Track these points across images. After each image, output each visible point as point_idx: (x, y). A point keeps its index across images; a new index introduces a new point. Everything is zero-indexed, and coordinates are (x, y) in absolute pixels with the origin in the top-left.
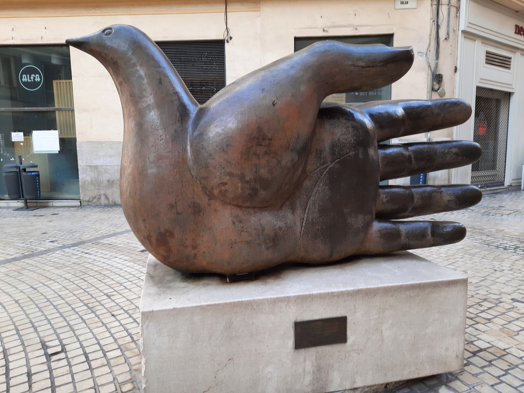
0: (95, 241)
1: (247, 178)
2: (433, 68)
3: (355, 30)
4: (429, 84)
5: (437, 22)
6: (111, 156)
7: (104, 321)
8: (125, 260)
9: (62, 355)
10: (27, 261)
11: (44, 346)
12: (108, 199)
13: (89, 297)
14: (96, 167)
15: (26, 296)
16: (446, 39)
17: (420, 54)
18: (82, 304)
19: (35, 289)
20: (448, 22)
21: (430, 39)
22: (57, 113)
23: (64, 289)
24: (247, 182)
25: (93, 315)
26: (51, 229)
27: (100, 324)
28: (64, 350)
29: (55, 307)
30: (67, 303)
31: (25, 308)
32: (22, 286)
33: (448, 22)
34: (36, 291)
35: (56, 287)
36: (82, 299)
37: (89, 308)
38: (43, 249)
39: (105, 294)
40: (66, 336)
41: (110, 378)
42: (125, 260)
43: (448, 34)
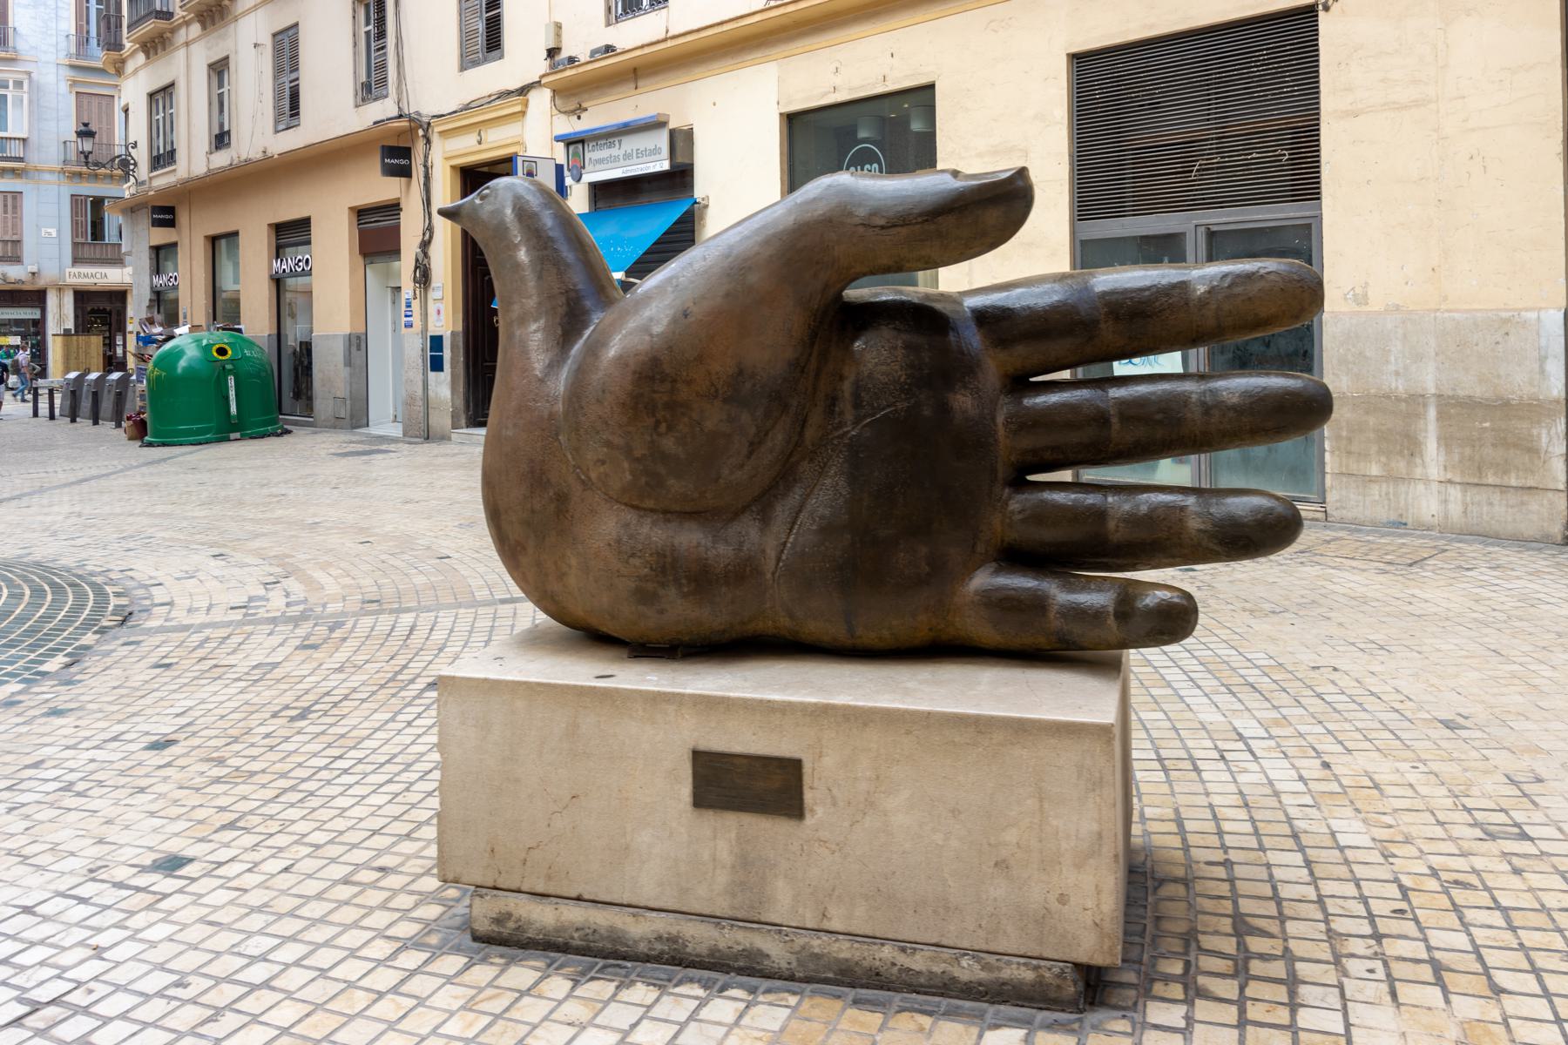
1: (638, 453)
24: (638, 460)
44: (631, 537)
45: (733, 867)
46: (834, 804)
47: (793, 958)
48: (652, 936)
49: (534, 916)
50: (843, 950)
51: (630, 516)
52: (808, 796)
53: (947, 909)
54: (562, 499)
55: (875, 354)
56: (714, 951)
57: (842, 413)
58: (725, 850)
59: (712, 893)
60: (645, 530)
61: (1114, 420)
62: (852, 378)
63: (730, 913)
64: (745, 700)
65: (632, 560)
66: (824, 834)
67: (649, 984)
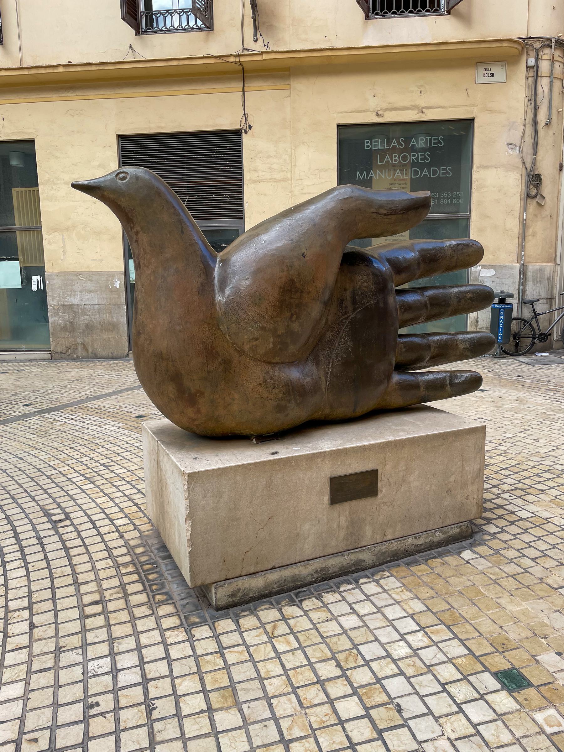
0: (79, 404)
2: (529, 165)
3: (420, 114)
4: (523, 188)
5: (535, 101)
6: (90, 292)
7: (105, 491)
8: (119, 428)
9: (68, 522)
11: (47, 514)
12: (87, 350)
13: (85, 467)
14: (71, 306)
15: (12, 466)
16: (546, 124)
17: (510, 146)
18: (77, 474)
19: (21, 458)
20: (550, 100)
21: (524, 125)
22: (18, 233)
23: (53, 459)
25: (92, 486)
26: (21, 390)
27: (102, 494)
28: (67, 517)
29: (49, 477)
30: (60, 472)
31: (16, 478)
33: (550, 100)
34: (22, 461)
35: (43, 456)
36: (77, 469)
37: (86, 478)
39: (102, 465)
40: (69, 505)
41: (121, 542)
42: (119, 428)
43: (550, 118)
44: (271, 378)
45: (347, 527)
46: (390, 485)
47: (375, 557)
48: (313, 572)
49: (253, 585)
50: (395, 546)
51: (267, 368)
53: (430, 515)
54: (227, 363)
55: (362, 280)
57: (346, 307)
58: (343, 521)
59: (338, 542)
60: (277, 374)
62: (351, 289)
64: (354, 448)
66: (385, 500)
67: (328, 592)
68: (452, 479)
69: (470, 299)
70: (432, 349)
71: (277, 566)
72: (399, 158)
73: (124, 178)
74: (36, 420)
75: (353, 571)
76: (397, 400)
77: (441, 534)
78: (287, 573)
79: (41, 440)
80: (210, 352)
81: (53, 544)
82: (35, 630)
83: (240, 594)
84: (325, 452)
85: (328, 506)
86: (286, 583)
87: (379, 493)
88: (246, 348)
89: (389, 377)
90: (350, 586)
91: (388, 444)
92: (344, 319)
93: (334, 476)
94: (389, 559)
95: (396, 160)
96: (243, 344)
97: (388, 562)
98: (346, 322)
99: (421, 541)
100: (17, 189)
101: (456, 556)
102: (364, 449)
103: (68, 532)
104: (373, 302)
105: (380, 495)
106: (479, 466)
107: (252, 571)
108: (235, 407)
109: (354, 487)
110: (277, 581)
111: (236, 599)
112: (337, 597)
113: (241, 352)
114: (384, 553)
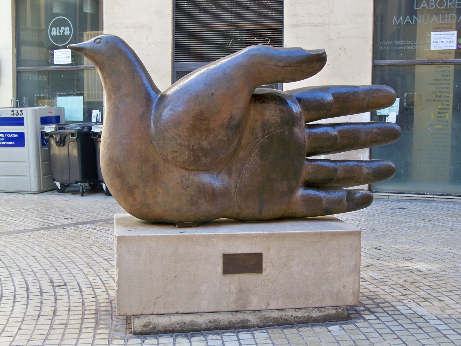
9: (64, 287)
10: (43, 231)
22: (85, 71)
23: (72, 253)
28: (65, 285)
32: (38, 249)
38: (58, 224)
40: (69, 279)
44: (187, 180)
45: (237, 293)
48: (207, 321)
51: (184, 172)
52: (264, 265)
56: (230, 322)
57: (257, 134)
58: (233, 287)
59: (229, 303)
61: (338, 137)
63: (235, 309)
65: (188, 189)
68: (330, 269)
69: (376, 133)
70: (339, 172)
71: (180, 312)
72: (435, 3)
73: (99, 42)
74: (71, 230)
75: (240, 327)
76: (299, 209)
77: (318, 312)
78: (188, 319)
79: (68, 241)
80: (145, 160)
81: (48, 297)
82: (20, 331)
83: (151, 326)
84: (220, 235)
85: (221, 275)
86: (186, 325)
87: (264, 272)
88: (170, 157)
89: (291, 191)
90: (233, 334)
91: (272, 235)
92: (255, 142)
93: (226, 253)
94: (271, 323)
95: (432, 6)
96: (167, 155)
97: (270, 326)
98: (256, 145)
99: (300, 314)
100: (88, 33)
101: (325, 328)
102: (252, 236)
103: (61, 293)
104: (279, 131)
105: (264, 273)
106: (355, 263)
107: (161, 312)
108: (160, 199)
109: (240, 264)
110: (179, 322)
111: (148, 329)
112: (219, 337)
113: (166, 160)
114: (266, 318)
